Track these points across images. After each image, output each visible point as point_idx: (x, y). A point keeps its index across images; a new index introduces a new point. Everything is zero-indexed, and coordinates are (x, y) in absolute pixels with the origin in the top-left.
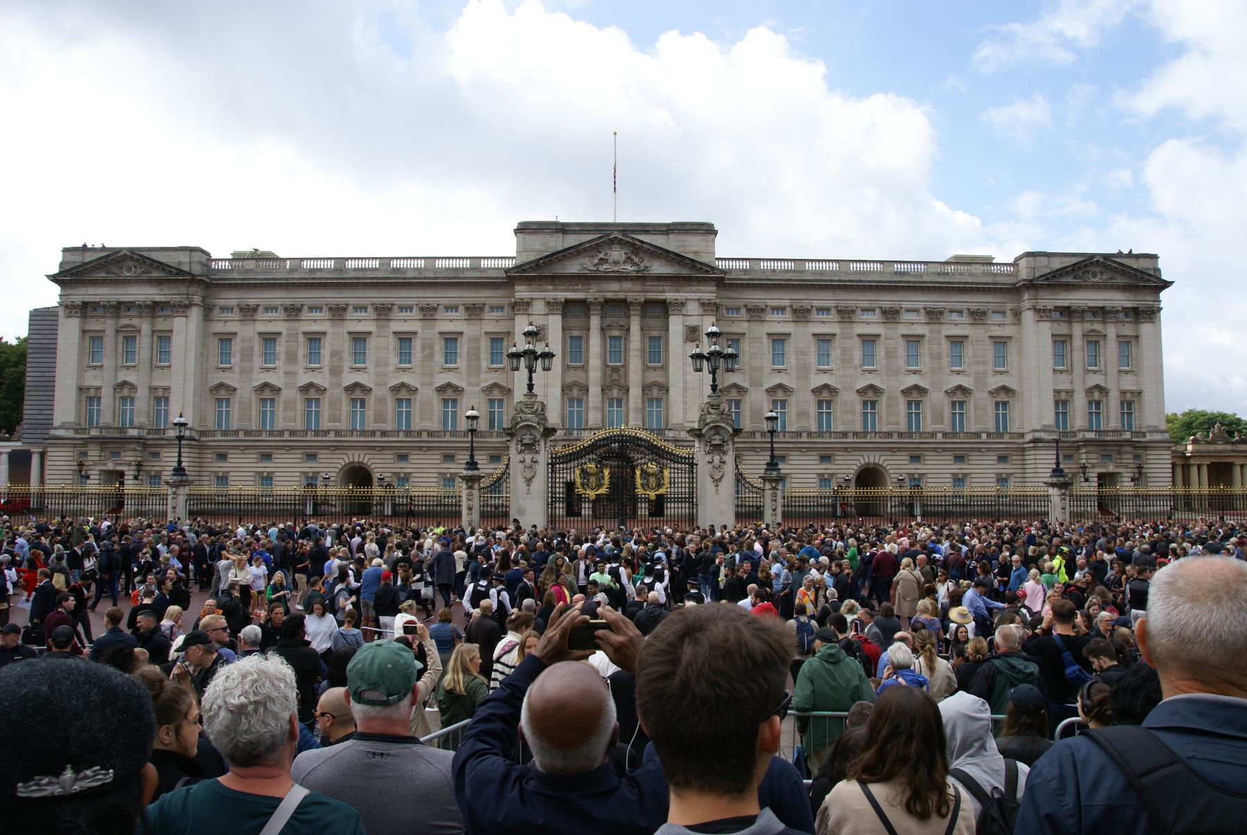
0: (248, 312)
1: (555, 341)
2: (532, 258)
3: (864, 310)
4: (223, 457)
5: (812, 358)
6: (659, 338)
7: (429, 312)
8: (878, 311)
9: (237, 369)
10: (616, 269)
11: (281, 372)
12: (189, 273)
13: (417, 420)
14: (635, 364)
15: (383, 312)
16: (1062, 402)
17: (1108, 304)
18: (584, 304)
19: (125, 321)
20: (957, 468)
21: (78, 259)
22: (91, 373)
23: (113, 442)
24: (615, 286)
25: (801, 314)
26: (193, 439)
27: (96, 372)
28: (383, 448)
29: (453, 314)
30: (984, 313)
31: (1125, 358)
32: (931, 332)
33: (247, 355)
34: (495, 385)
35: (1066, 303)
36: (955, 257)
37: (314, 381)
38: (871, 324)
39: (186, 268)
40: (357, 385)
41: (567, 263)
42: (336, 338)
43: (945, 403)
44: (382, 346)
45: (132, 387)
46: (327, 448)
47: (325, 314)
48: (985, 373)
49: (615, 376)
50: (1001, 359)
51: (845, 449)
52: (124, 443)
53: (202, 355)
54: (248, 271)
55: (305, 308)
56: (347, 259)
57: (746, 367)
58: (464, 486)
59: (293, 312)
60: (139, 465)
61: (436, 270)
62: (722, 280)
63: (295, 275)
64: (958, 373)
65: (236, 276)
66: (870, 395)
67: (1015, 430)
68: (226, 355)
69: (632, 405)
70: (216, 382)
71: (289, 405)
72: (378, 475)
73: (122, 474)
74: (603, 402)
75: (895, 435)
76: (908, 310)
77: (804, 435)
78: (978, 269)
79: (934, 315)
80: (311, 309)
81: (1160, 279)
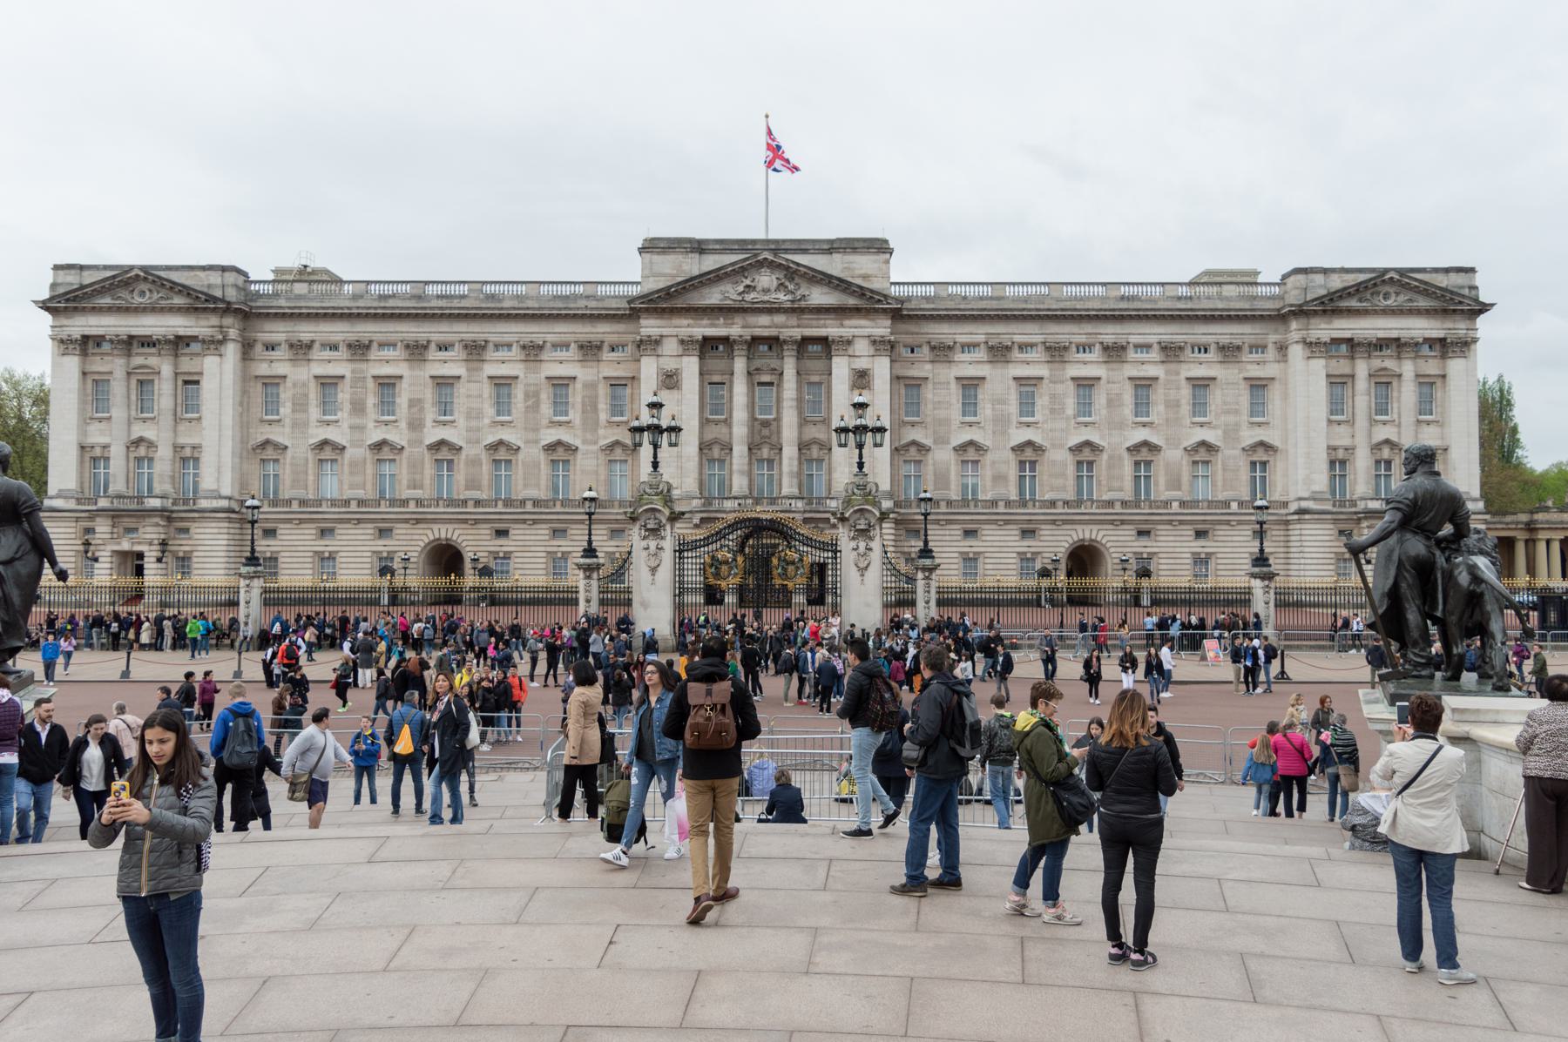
0: (301, 349)
1: (684, 407)
2: (661, 285)
4: (270, 533)
5: (1013, 408)
6: (820, 384)
7: (532, 351)
9: (287, 421)
10: (766, 298)
11: (345, 425)
12: (222, 300)
13: (520, 487)
14: (789, 419)
15: (475, 350)
16: (1338, 463)
17: (1404, 335)
18: (725, 340)
19: (138, 361)
20: (1199, 546)
21: (72, 279)
22: (94, 427)
23: (126, 515)
24: (764, 320)
25: (999, 353)
26: (233, 511)
27: (103, 425)
28: (477, 521)
29: (562, 354)
30: (1239, 348)
31: (1426, 404)
32: (1167, 373)
33: (300, 405)
34: (617, 443)
35: (1347, 334)
36: (1207, 273)
37: (390, 437)
38: (1090, 365)
39: (218, 294)
41: (706, 291)
42: (414, 382)
43: (1185, 462)
44: (473, 394)
45: (151, 445)
46: (406, 521)
47: (398, 353)
48: (1237, 425)
49: (766, 432)
50: (1258, 407)
51: (1054, 522)
52: (144, 517)
53: (241, 404)
54: (299, 297)
55: (375, 345)
56: (427, 283)
57: (929, 420)
58: (581, 574)
59: (359, 349)
60: (164, 543)
61: (538, 298)
62: (899, 313)
63: (361, 303)
65: (282, 303)
66: (1086, 454)
67: (1276, 497)
68: (271, 405)
69: (785, 468)
70: (261, 439)
71: (356, 466)
72: (471, 555)
73: (140, 556)
74: (750, 463)
75: (1118, 505)
76: (1137, 346)
77: (1001, 504)
78: (1230, 291)
79: (1171, 352)
80: (382, 345)
81: (1476, 300)
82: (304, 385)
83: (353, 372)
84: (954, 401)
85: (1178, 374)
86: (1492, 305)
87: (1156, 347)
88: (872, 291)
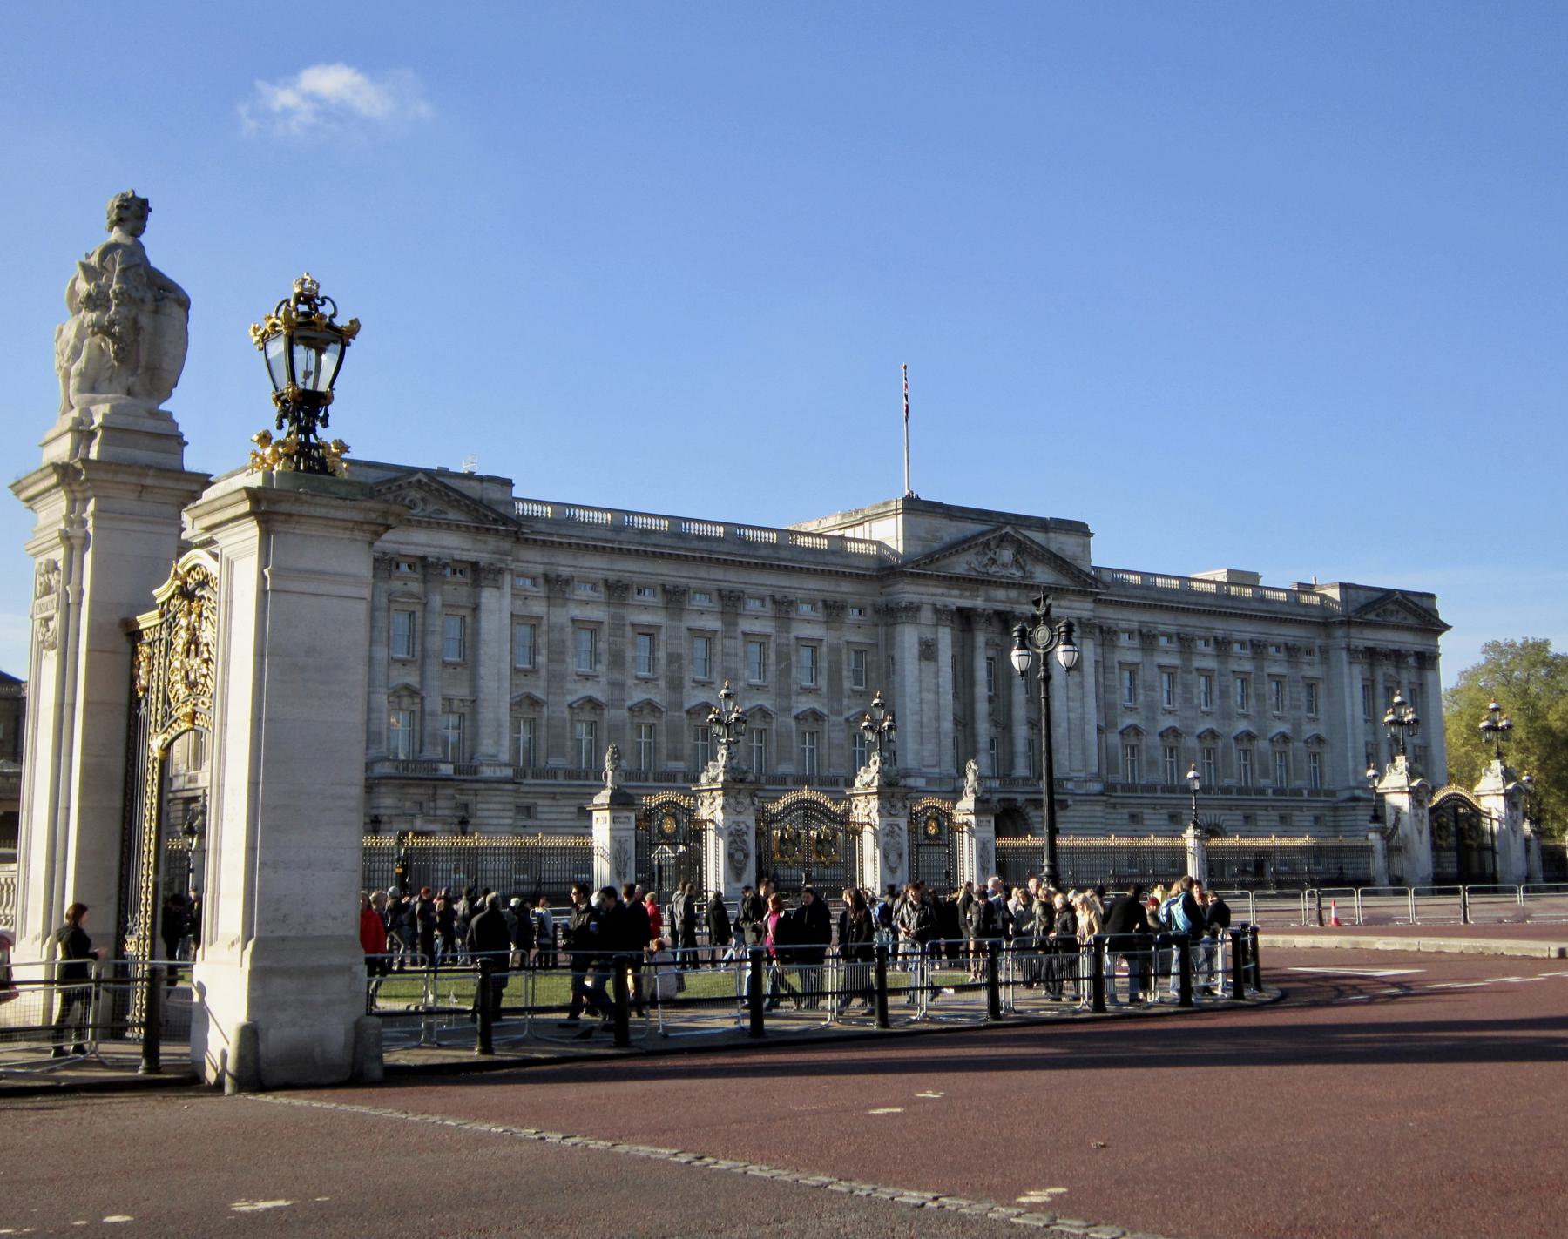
0: (556, 586)
7: (783, 607)
10: (1003, 572)
11: (603, 680)
13: (774, 761)
15: (731, 602)
17: (1403, 648)
24: (1001, 594)
25: (1147, 639)
33: (557, 654)
35: (1370, 644)
41: (954, 559)
47: (659, 600)
64: (1279, 718)
76: (1237, 642)
79: (1258, 648)
82: (562, 629)
83: (613, 617)
86: (1446, 627)
88: (1088, 575)
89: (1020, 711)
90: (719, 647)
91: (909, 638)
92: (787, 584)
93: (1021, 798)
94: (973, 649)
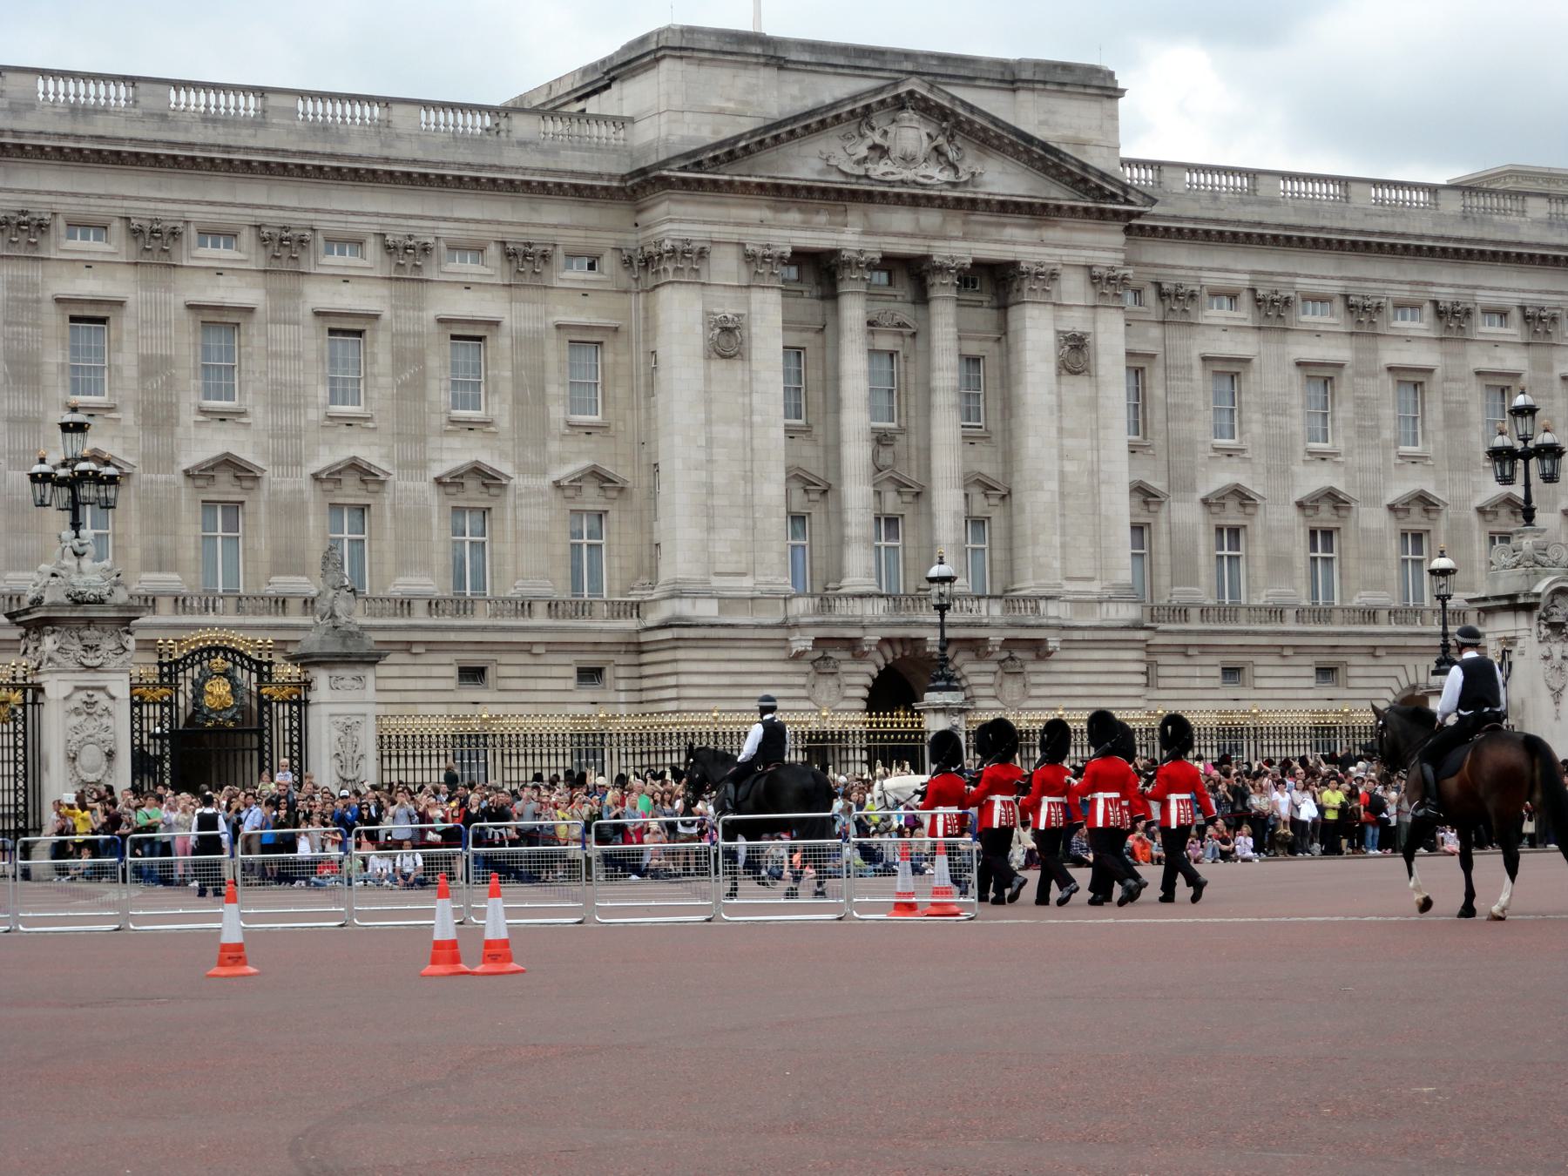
3: (1400, 306)
5: (1297, 424)
7: (408, 257)
8: (1428, 309)
10: (908, 175)
15: (285, 248)
24: (901, 219)
25: (1273, 310)
32: (1534, 364)
40: (228, 463)
41: (792, 148)
44: (286, 349)
47: (115, 246)
49: (886, 456)
51: (1372, 651)
57: (1159, 441)
61: (421, 137)
63: (28, 123)
76: (1488, 311)
77: (1290, 613)
83: (12, 285)
84: (1200, 405)
85: (1550, 368)
87: (1516, 315)
88: (1103, 176)
89: (947, 460)
90: (258, 342)
91: (681, 314)
92: (417, 211)
93: (933, 636)
94: (838, 333)
